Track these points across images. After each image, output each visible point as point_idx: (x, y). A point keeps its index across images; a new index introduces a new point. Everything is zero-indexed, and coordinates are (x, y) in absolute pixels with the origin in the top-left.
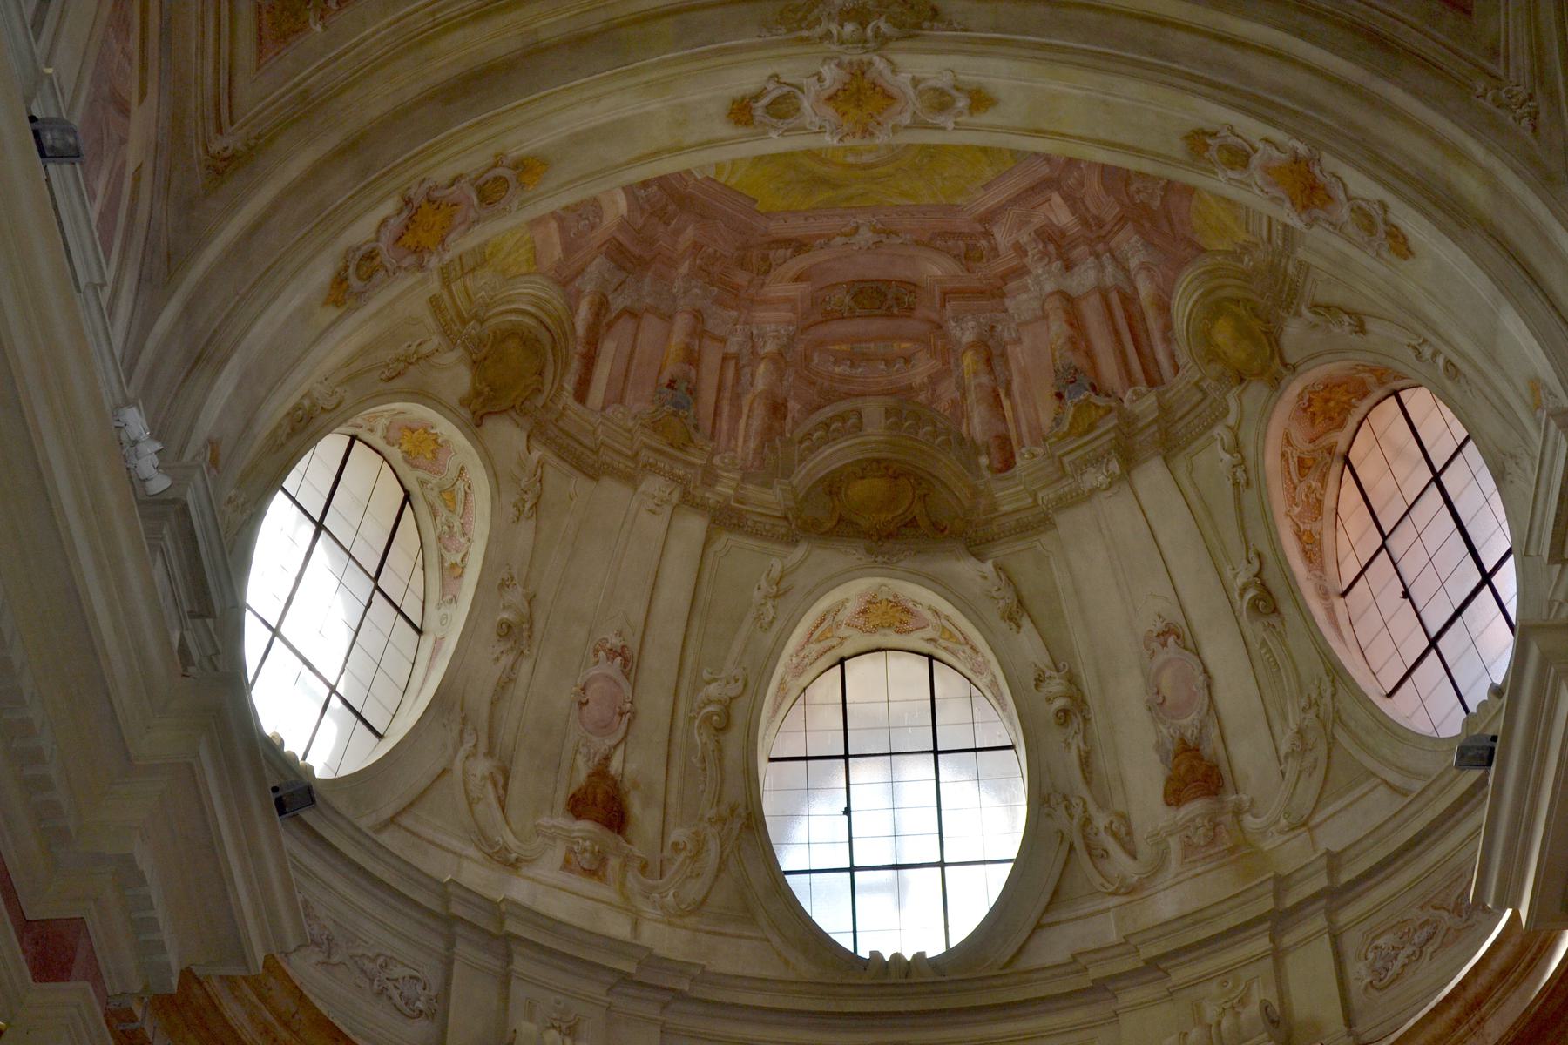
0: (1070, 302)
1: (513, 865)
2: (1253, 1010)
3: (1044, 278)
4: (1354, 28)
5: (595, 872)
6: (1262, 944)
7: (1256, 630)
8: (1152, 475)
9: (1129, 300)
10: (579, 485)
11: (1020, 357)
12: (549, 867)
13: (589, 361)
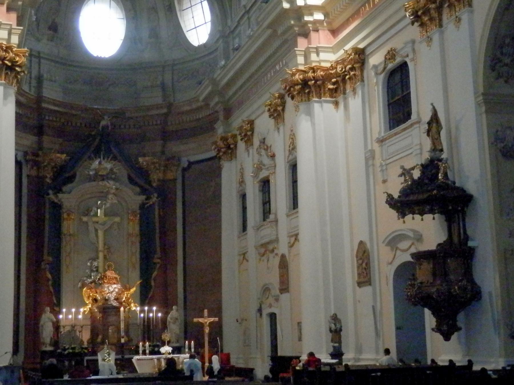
2: (159, 83)
5: (52, 41)
12: (45, 41)
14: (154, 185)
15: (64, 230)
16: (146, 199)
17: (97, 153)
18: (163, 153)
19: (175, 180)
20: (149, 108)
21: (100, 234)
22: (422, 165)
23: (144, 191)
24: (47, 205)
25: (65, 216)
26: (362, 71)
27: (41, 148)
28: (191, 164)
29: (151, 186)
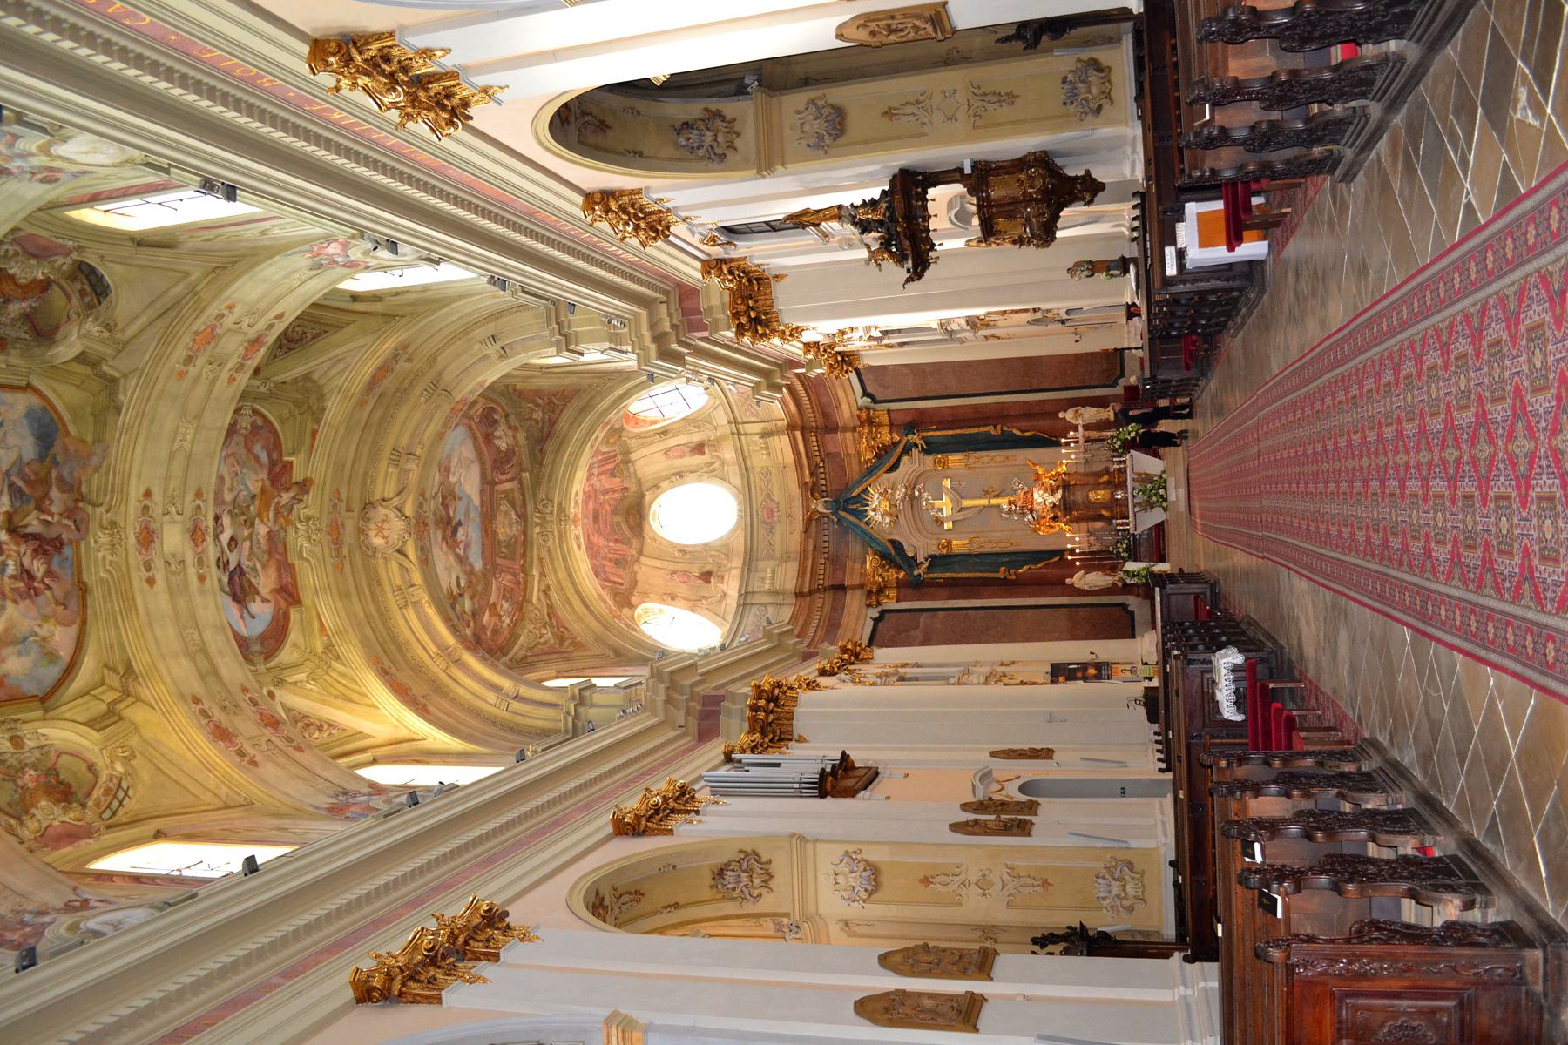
0: (599, 474)
1: (724, 595)
3: (594, 480)
4: (579, 415)
5: (723, 578)
6: (743, 438)
7: (670, 435)
8: (633, 456)
9: (601, 461)
10: (639, 584)
11: (607, 486)
12: (724, 587)
13: (615, 583)
14: (896, 437)
15: (966, 550)
16: (916, 446)
17: (861, 514)
18: (854, 429)
19: (889, 411)
20: (796, 453)
21: (966, 503)
22: (862, 233)
23: (907, 450)
24: (931, 575)
25: (944, 552)
26: (732, 260)
27: (861, 586)
28: (866, 394)
29: (899, 442)
